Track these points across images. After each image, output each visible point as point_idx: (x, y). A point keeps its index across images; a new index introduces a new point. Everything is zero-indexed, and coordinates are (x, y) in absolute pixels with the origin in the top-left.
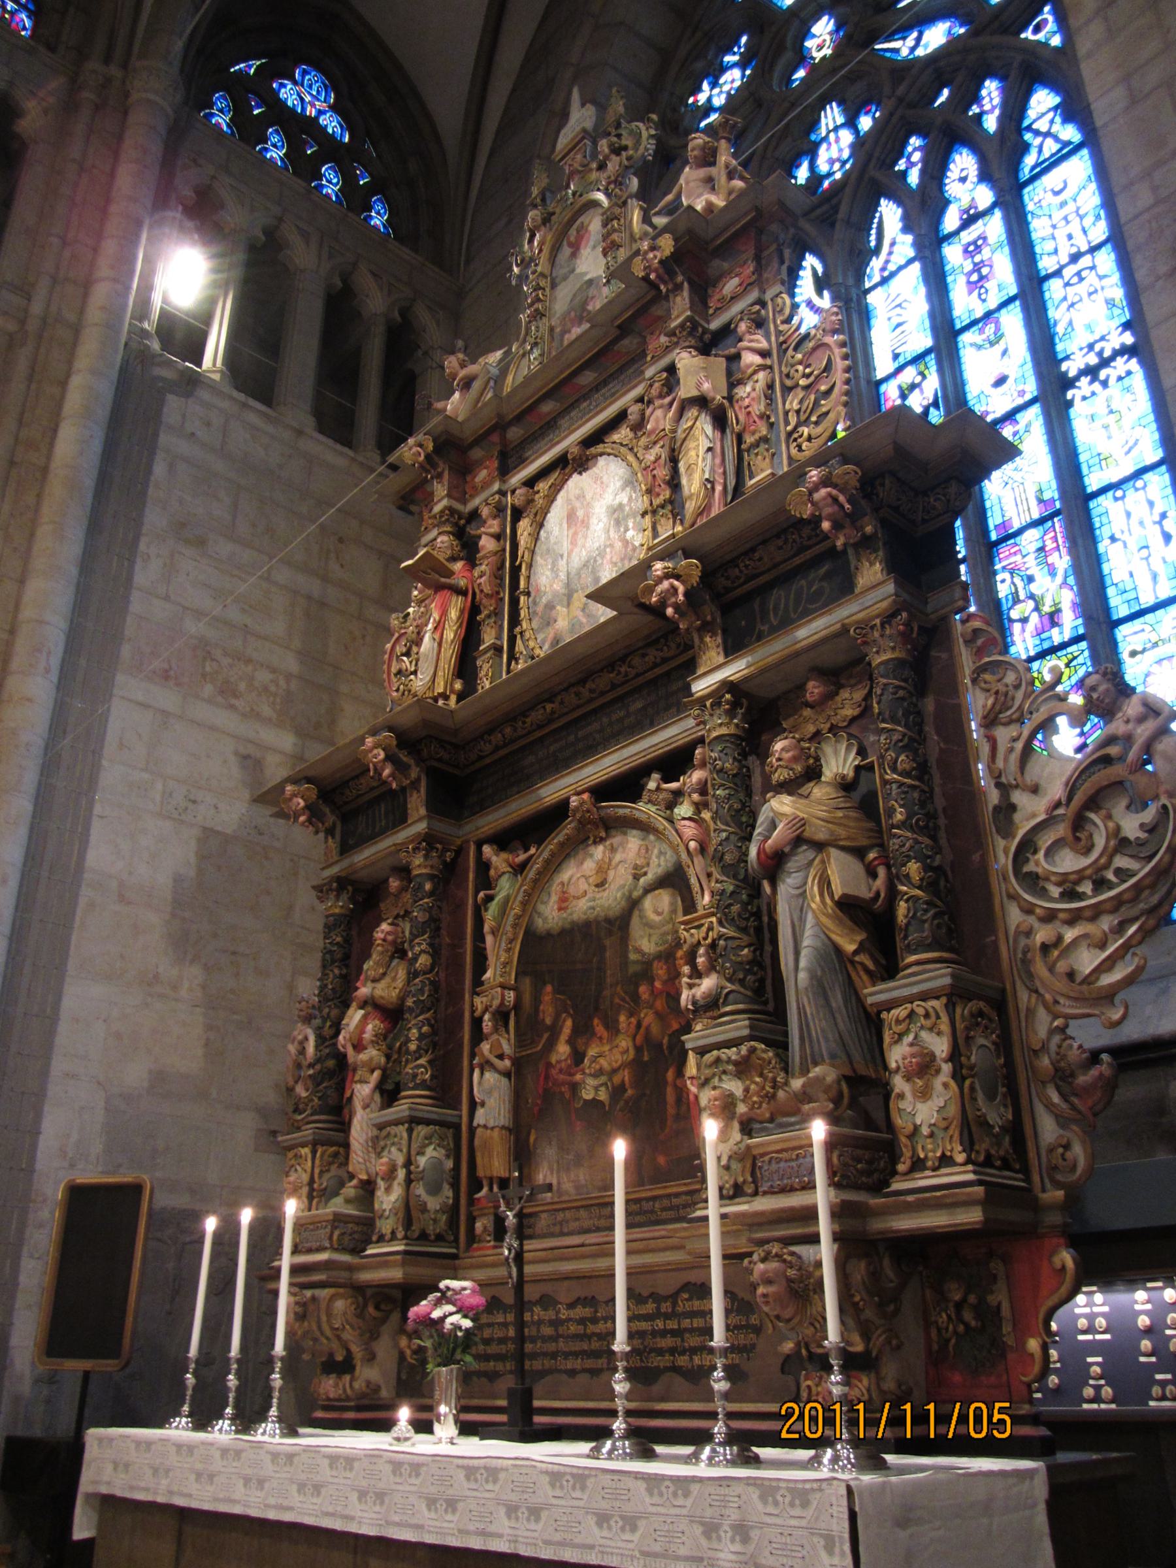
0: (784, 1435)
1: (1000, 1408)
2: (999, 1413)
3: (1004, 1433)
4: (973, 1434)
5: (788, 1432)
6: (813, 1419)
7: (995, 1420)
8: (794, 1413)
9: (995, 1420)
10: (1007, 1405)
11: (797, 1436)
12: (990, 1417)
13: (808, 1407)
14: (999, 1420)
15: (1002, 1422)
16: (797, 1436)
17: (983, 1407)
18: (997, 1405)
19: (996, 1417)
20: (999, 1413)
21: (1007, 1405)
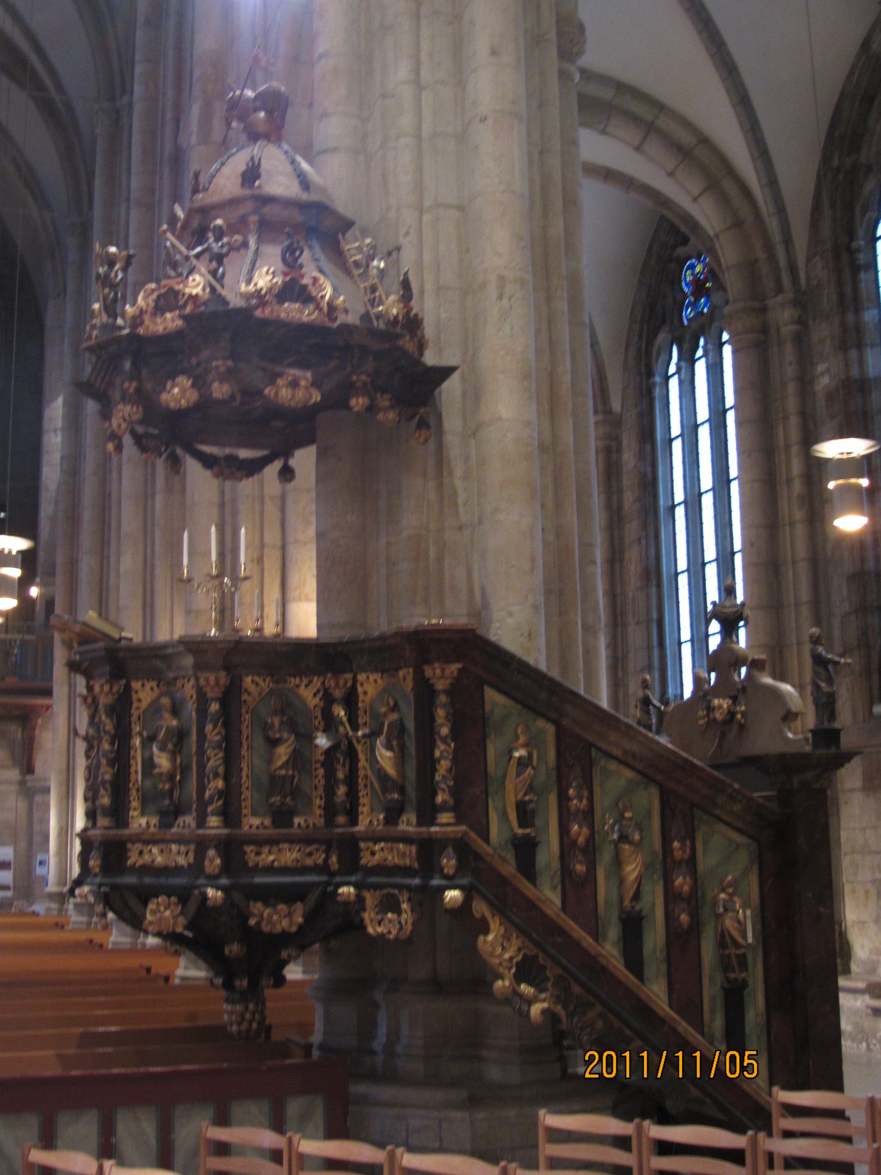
0: (587, 1075)
1: (749, 1055)
2: (748, 1059)
3: (752, 1074)
4: (729, 1074)
5: (590, 1073)
6: (609, 1064)
7: (745, 1064)
8: (595, 1059)
9: (745, 1064)
10: (755, 1053)
12: (742, 1060)
13: (605, 1054)
14: (748, 1064)
16: (597, 1076)
17: (737, 1054)
18: (747, 1053)
20: (748, 1059)
21: (755, 1053)
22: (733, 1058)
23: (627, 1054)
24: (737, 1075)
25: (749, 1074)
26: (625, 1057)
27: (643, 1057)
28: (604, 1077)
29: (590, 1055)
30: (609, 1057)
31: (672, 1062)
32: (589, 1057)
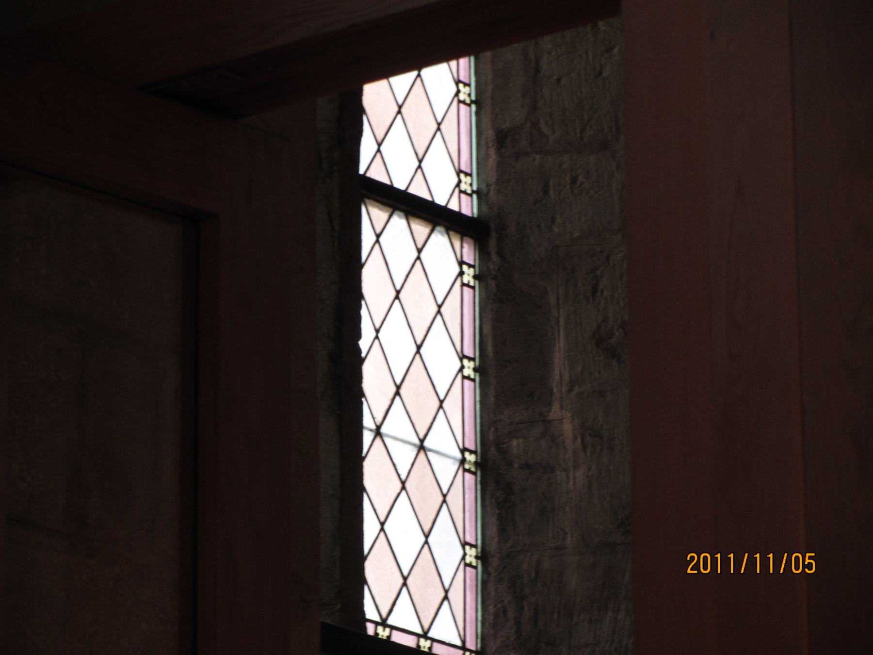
0: (689, 571)
1: (809, 556)
2: (809, 559)
5: (691, 570)
7: (806, 563)
9: (806, 563)
10: (813, 554)
11: (696, 572)
12: (804, 561)
13: (702, 556)
14: (808, 563)
15: (810, 564)
16: (696, 572)
18: (808, 555)
19: (807, 561)
20: (809, 559)
21: (813, 554)
22: (797, 558)
23: (719, 556)
24: (800, 571)
25: (809, 570)
26: (730, 557)
27: (730, 557)
28: (701, 572)
29: (691, 556)
30: (705, 558)
31: (752, 562)
32: (690, 558)
